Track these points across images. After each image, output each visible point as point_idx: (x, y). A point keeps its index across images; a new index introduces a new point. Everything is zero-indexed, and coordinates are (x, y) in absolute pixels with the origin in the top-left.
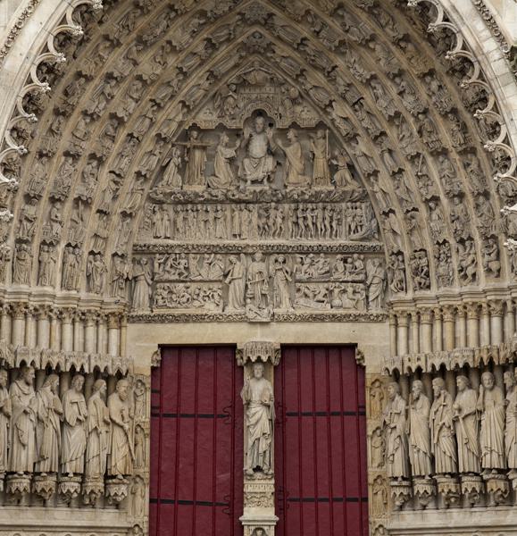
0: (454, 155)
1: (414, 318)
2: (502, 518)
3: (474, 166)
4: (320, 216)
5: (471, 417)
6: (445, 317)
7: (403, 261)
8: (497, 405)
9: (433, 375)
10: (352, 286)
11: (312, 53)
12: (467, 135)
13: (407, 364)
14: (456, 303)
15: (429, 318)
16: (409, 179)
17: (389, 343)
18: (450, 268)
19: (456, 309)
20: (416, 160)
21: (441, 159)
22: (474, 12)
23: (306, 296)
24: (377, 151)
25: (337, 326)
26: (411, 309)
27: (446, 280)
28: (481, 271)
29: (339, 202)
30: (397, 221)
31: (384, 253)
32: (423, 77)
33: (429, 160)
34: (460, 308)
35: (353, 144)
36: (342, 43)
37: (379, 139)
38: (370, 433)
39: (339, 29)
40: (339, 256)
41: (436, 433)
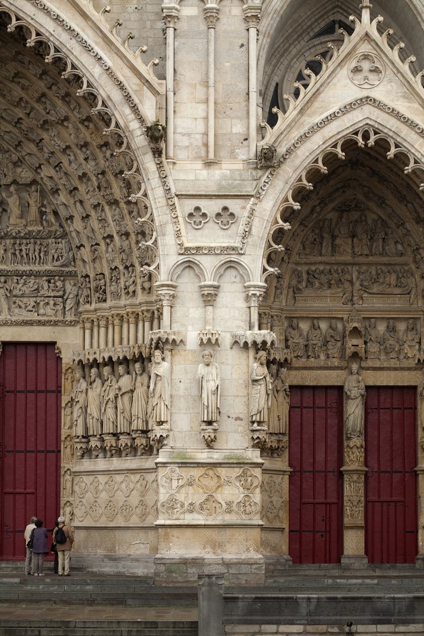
0: (123, 205)
1: (95, 323)
2: (144, 464)
3: (135, 213)
4: (32, 249)
5: (127, 394)
6: (115, 322)
7: (90, 282)
8: (143, 386)
9: (105, 364)
10: (54, 300)
11: (26, 129)
12: (130, 190)
13: (87, 356)
14: (123, 312)
15: (105, 323)
16: (94, 223)
17: (79, 341)
18: (119, 287)
19: (123, 316)
20: (98, 208)
21: (114, 207)
22: (123, 101)
23: (20, 307)
24: (72, 201)
25: (42, 328)
26: (93, 316)
27: (117, 296)
28: (139, 287)
29: (47, 238)
30: (85, 252)
31: (77, 276)
32: (100, 147)
33: (107, 208)
34: (125, 316)
35: (56, 196)
36: (46, 122)
37: (73, 193)
38: (63, 405)
39: (43, 112)
40: (45, 278)
41: (104, 405)
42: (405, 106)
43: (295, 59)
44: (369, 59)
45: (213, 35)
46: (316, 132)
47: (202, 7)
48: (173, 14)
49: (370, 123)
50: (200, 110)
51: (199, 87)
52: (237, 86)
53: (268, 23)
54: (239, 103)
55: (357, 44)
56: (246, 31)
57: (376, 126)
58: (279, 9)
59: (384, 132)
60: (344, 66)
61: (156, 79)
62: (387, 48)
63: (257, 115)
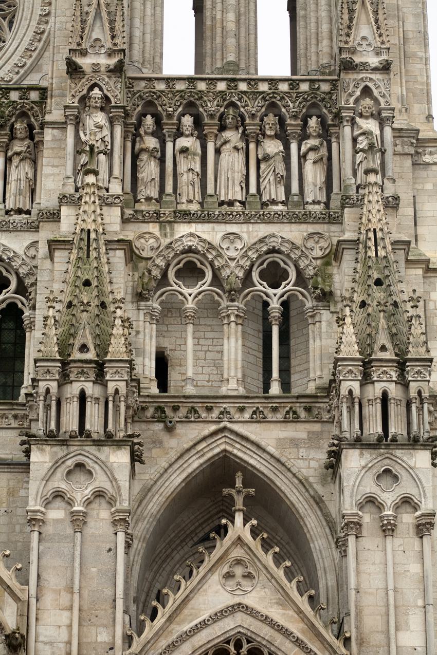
42: (279, 614)
43: (178, 565)
44: (242, 565)
45: (79, 538)
46: (185, 641)
47: (69, 510)
48: (38, 517)
49: (242, 631)
50: (64, 618)
51: (63, 593)
52: (103, 592)
53: (142, 529)
54: (105, 610)
55: (228, 549)
56: (114, 535)
57: (249, 635)
58: (155, 513)
59: (257, 641)
60: (216, 571)
61: (18, 584)
62: (260, 552)
63: (124, 622)
